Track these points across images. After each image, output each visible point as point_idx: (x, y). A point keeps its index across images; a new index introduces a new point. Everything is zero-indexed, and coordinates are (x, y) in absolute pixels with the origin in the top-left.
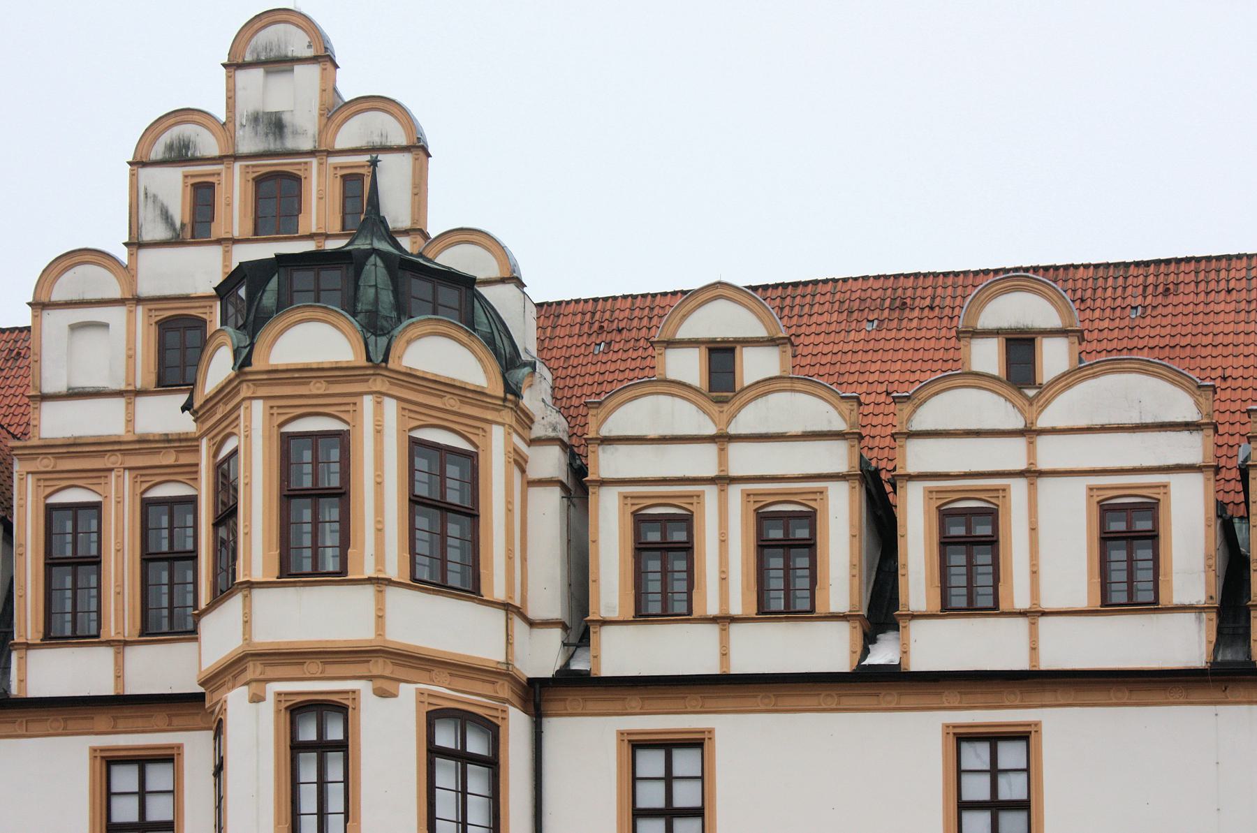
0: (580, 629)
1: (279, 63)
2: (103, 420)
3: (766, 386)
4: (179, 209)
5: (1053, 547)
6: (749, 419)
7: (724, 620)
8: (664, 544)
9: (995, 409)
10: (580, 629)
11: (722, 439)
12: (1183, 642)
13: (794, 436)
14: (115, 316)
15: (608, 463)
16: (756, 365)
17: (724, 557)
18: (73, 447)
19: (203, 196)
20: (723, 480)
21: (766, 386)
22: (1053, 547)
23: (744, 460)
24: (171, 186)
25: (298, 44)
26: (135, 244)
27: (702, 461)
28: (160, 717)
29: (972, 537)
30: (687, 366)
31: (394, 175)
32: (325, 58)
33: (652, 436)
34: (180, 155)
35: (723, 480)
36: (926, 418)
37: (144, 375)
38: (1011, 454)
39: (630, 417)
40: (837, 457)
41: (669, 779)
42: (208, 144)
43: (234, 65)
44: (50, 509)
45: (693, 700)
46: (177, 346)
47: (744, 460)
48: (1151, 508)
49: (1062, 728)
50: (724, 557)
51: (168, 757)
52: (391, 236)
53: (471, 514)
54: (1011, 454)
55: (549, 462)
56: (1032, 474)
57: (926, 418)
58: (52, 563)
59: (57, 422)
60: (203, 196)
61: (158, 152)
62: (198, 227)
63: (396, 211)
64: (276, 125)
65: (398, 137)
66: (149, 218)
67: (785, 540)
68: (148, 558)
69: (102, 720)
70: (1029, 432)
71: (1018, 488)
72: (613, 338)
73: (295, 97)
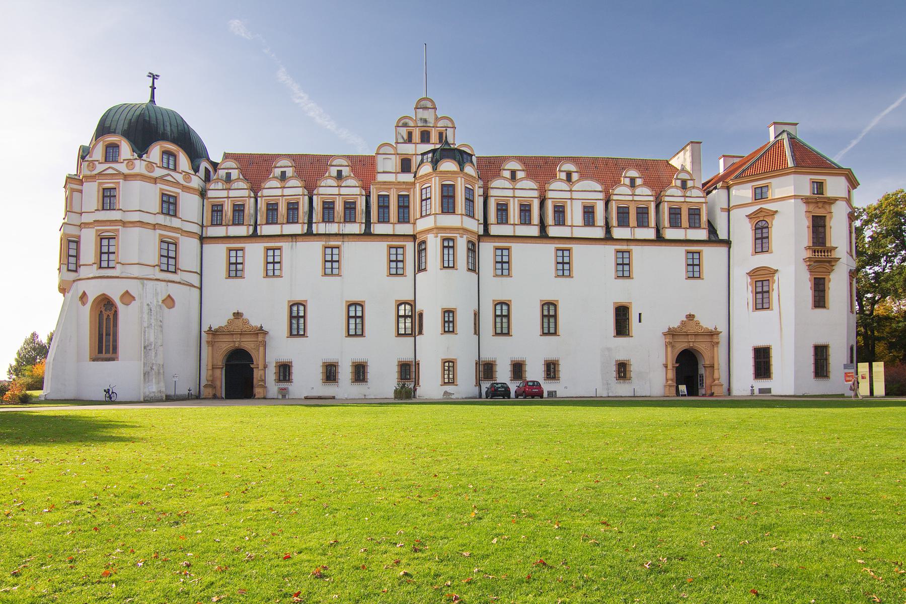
0: (486, 224)
1: (425, 108)
2: (390, 178)
3: (522, 179)
4: (406, 137)
5: (575, 214)
6: (518, 186)
7: (514, 225)
8: (503, 209)
9: (565, 186)
10: (486, 224)
11: (514, 189)
12: (599, 233)
13: (527, 189)
14: (393, 157)
15: (492, 192)
16: (520, 175)
17: (514, 213)
18: (385, 183)
19: (410, 134)
20: (514, 197)
21: (522, 179)
22: (575, 214)
23: (518, 193)
24: (404, 132)
25: (429, 105)
26: (397, 143)
27: (509, 193)
28: (402, 238)
29: (560, 211)
30: (507, 174)
31: (450, 132)
32: (435, 108)
33: (500, 188)
34: (405, 125)
35: (514, 197)
36: (552, 187)
37: (399, 170)
38: (568, 195)
39: (496, 183)
40: (535, 194)
41: (502, 256)
42: (411, 124)
43: (416, 108)
44: (379, 196)
45: (508, 239)
46: (406, 165)
47: (518, 193)
48: (593, 207)
49: (576, 248)
50: (514, 213)
51: (403, 247)
52: (449, 145)
53: (473, 201)
54: (568, 195)
55: (481, 191)
56: (571, 199)
57: (552, 187)
58: (379, 207)
59: (381, 178)
60: (410, 134)
61: (400, 124)
62: (410, 140)
63: (450, 140)
64: (425, 121)
65: (450, 125)
66: (399, 137)
67: (525, 210)
68: (399, 207)
69: (390, 239)
70: (570, 191)
71: (569, 201)
72: (490, 168)
73: (428, 115)
